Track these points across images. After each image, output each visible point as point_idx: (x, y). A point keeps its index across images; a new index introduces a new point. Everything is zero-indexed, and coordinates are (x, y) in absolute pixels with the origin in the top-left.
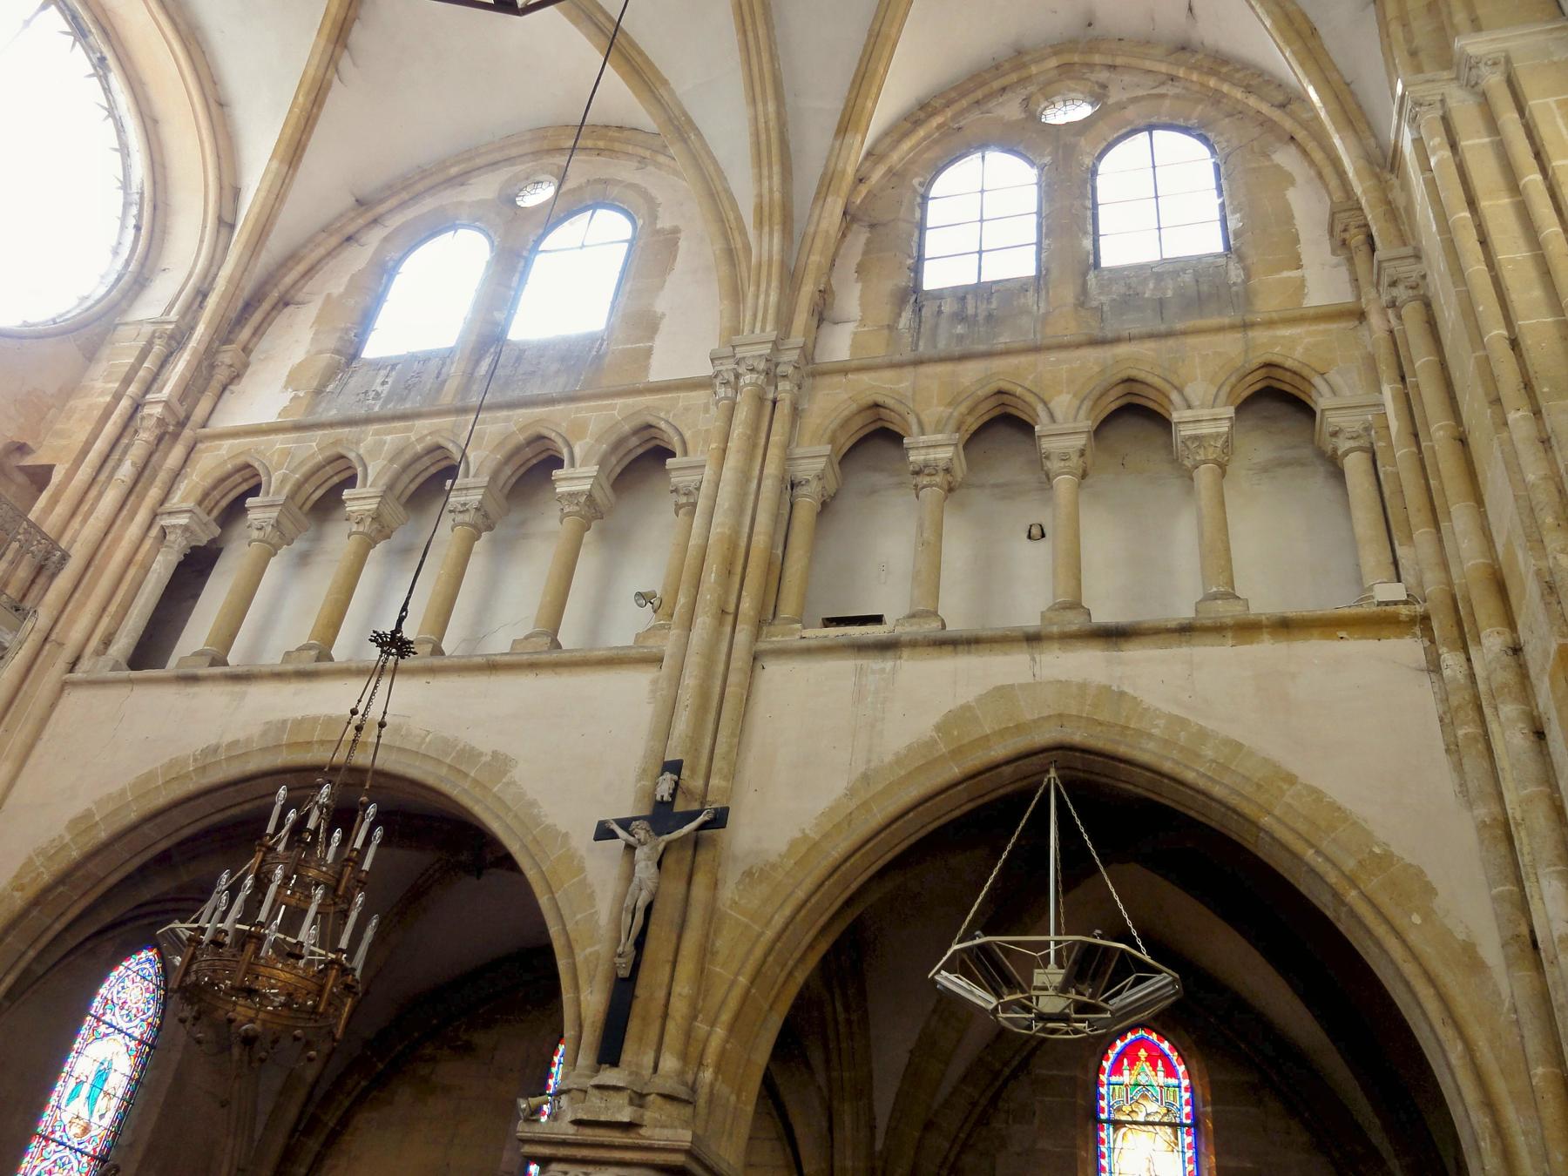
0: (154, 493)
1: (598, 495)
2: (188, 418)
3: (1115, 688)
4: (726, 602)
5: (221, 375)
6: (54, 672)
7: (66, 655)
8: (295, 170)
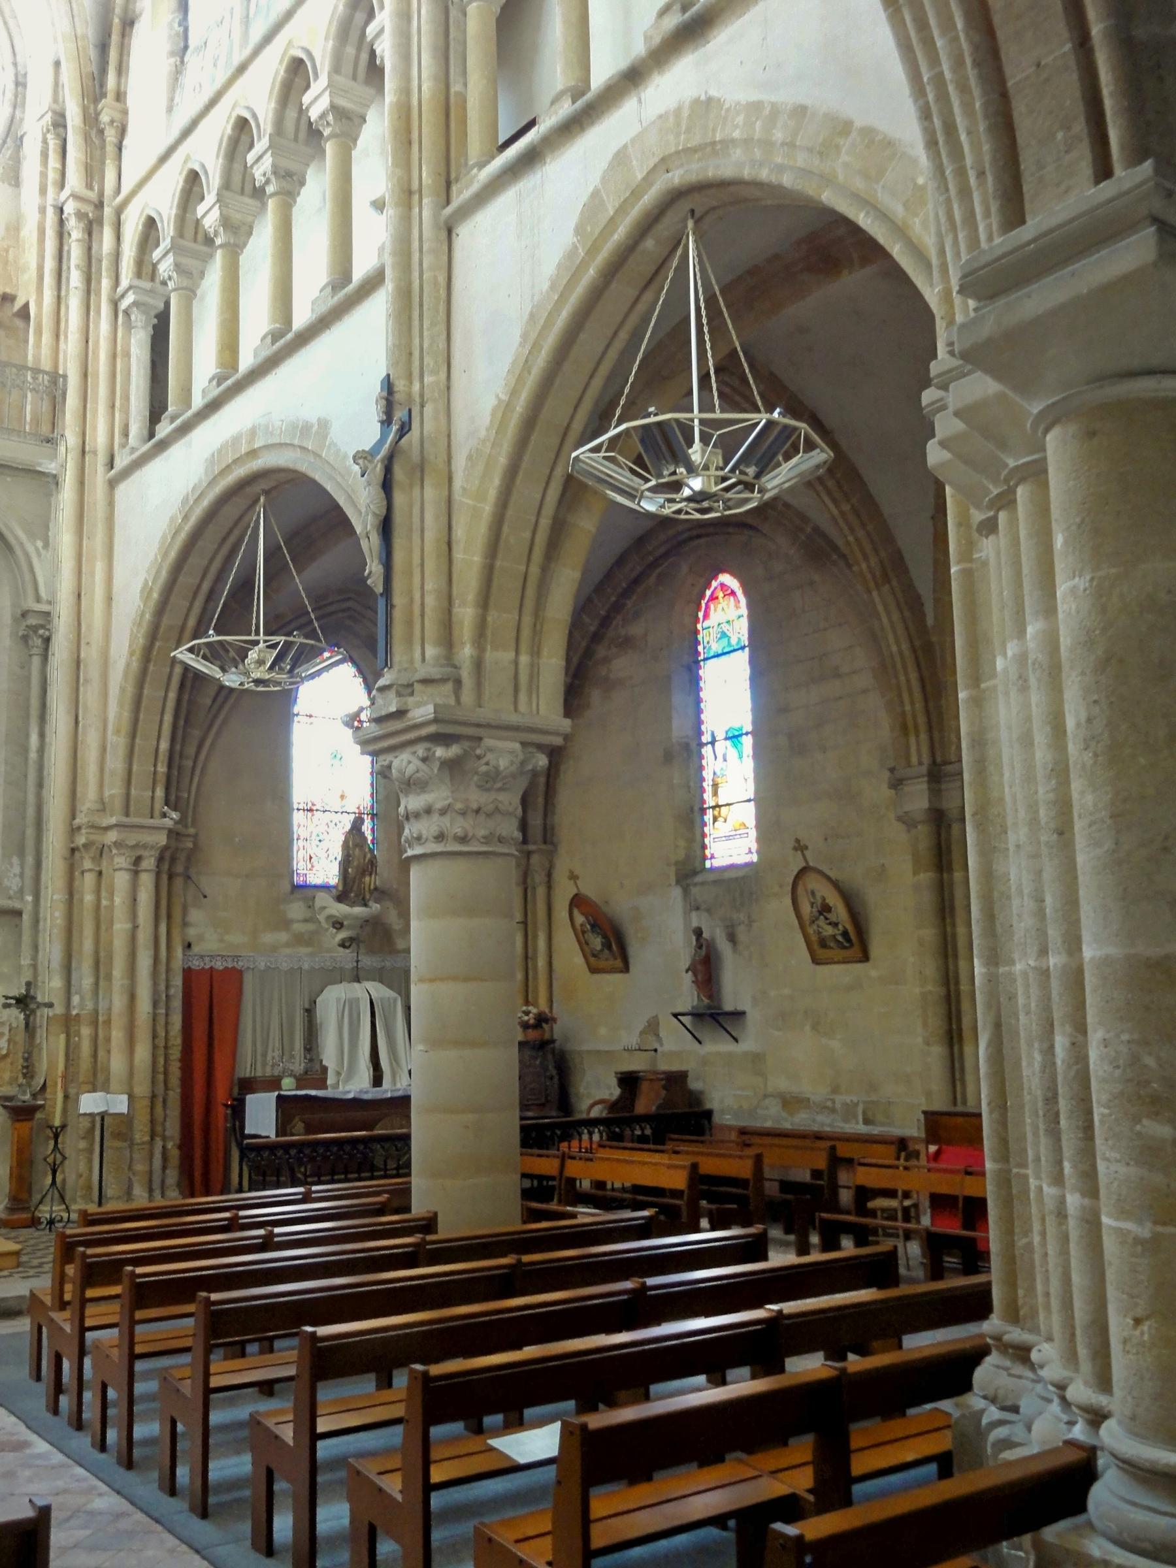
0: (106, 283)
1: (342, 102)
2: (101, 194)
4: (410, 180)
5: (111, 136)
7: (102, 458)
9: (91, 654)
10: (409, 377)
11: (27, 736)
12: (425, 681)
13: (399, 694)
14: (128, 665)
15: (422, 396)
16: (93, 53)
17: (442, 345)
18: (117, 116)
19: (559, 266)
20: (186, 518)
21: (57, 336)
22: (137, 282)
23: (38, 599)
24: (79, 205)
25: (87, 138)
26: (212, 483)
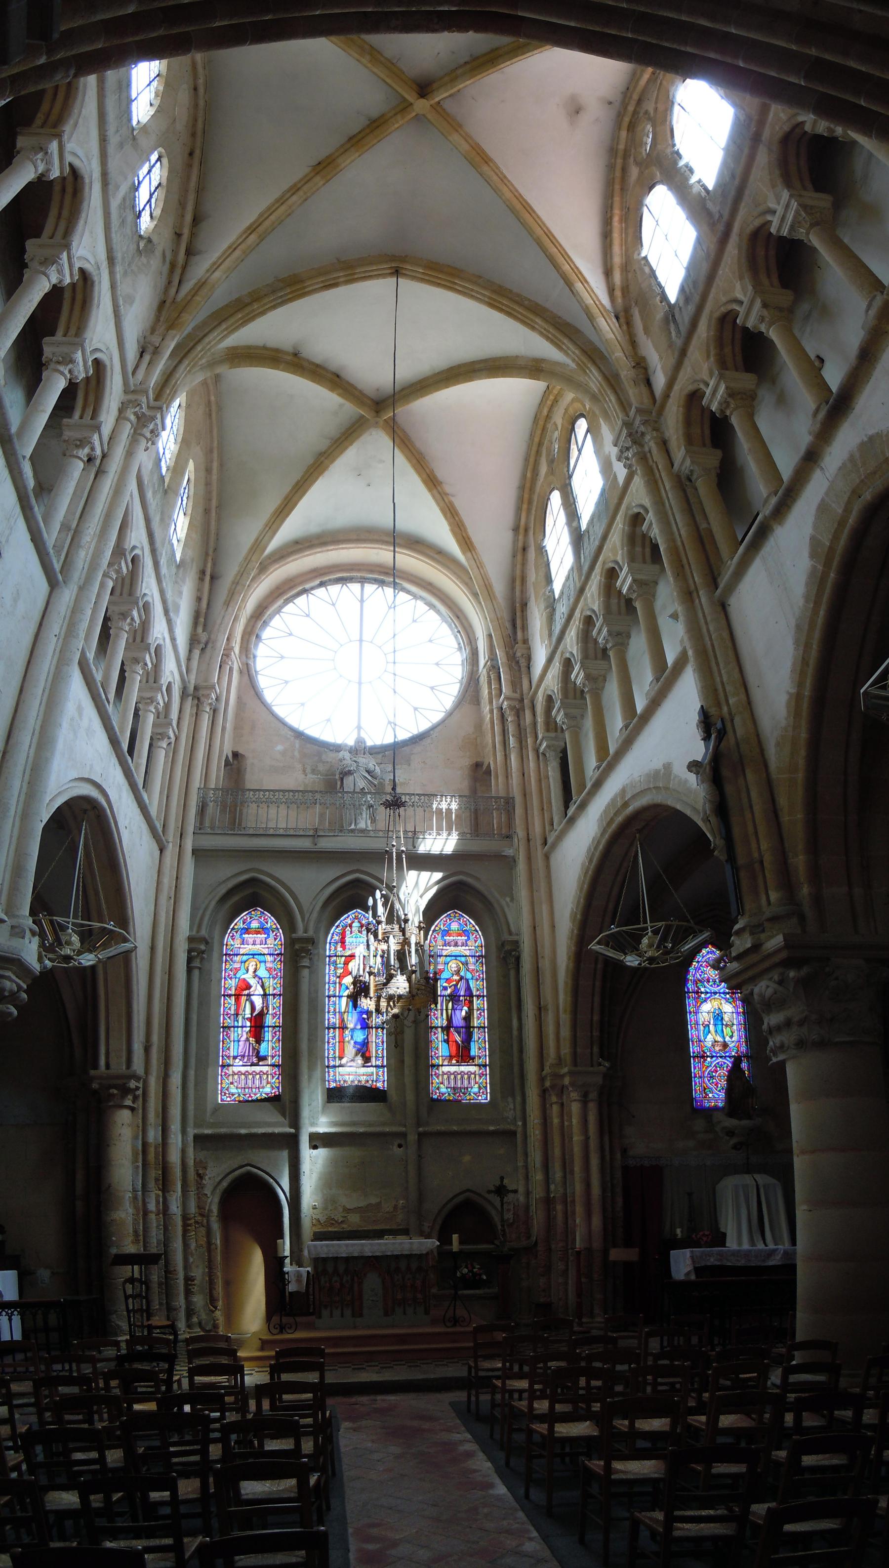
0: (530, 741)
1: (639, 577)
3: (865, 439)
6: (539, 854)
7: (539, 842)
8: (474, 548)
9: (545, 964)
10: (719, 705)
11: (511, 1021)
12: (774, 919)
13: (752, 934)
14: (567, 967)
15: (730, 713)
16: (508, 625)
17: (736, 675)
18: (525, 652)
19: (807, 584)
20: (591, 861)
21: (507, 777)
22: (547, 734)
23: (510, 933)
24: (510, 702)
25: (510, 668)
26: (602, 834)
